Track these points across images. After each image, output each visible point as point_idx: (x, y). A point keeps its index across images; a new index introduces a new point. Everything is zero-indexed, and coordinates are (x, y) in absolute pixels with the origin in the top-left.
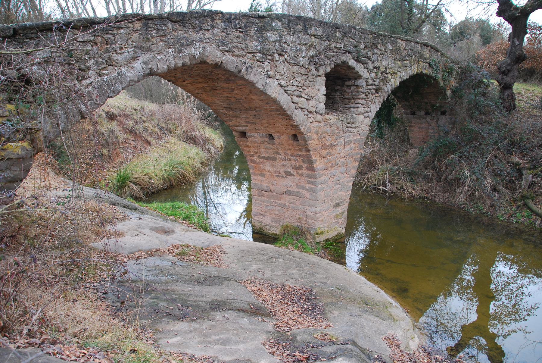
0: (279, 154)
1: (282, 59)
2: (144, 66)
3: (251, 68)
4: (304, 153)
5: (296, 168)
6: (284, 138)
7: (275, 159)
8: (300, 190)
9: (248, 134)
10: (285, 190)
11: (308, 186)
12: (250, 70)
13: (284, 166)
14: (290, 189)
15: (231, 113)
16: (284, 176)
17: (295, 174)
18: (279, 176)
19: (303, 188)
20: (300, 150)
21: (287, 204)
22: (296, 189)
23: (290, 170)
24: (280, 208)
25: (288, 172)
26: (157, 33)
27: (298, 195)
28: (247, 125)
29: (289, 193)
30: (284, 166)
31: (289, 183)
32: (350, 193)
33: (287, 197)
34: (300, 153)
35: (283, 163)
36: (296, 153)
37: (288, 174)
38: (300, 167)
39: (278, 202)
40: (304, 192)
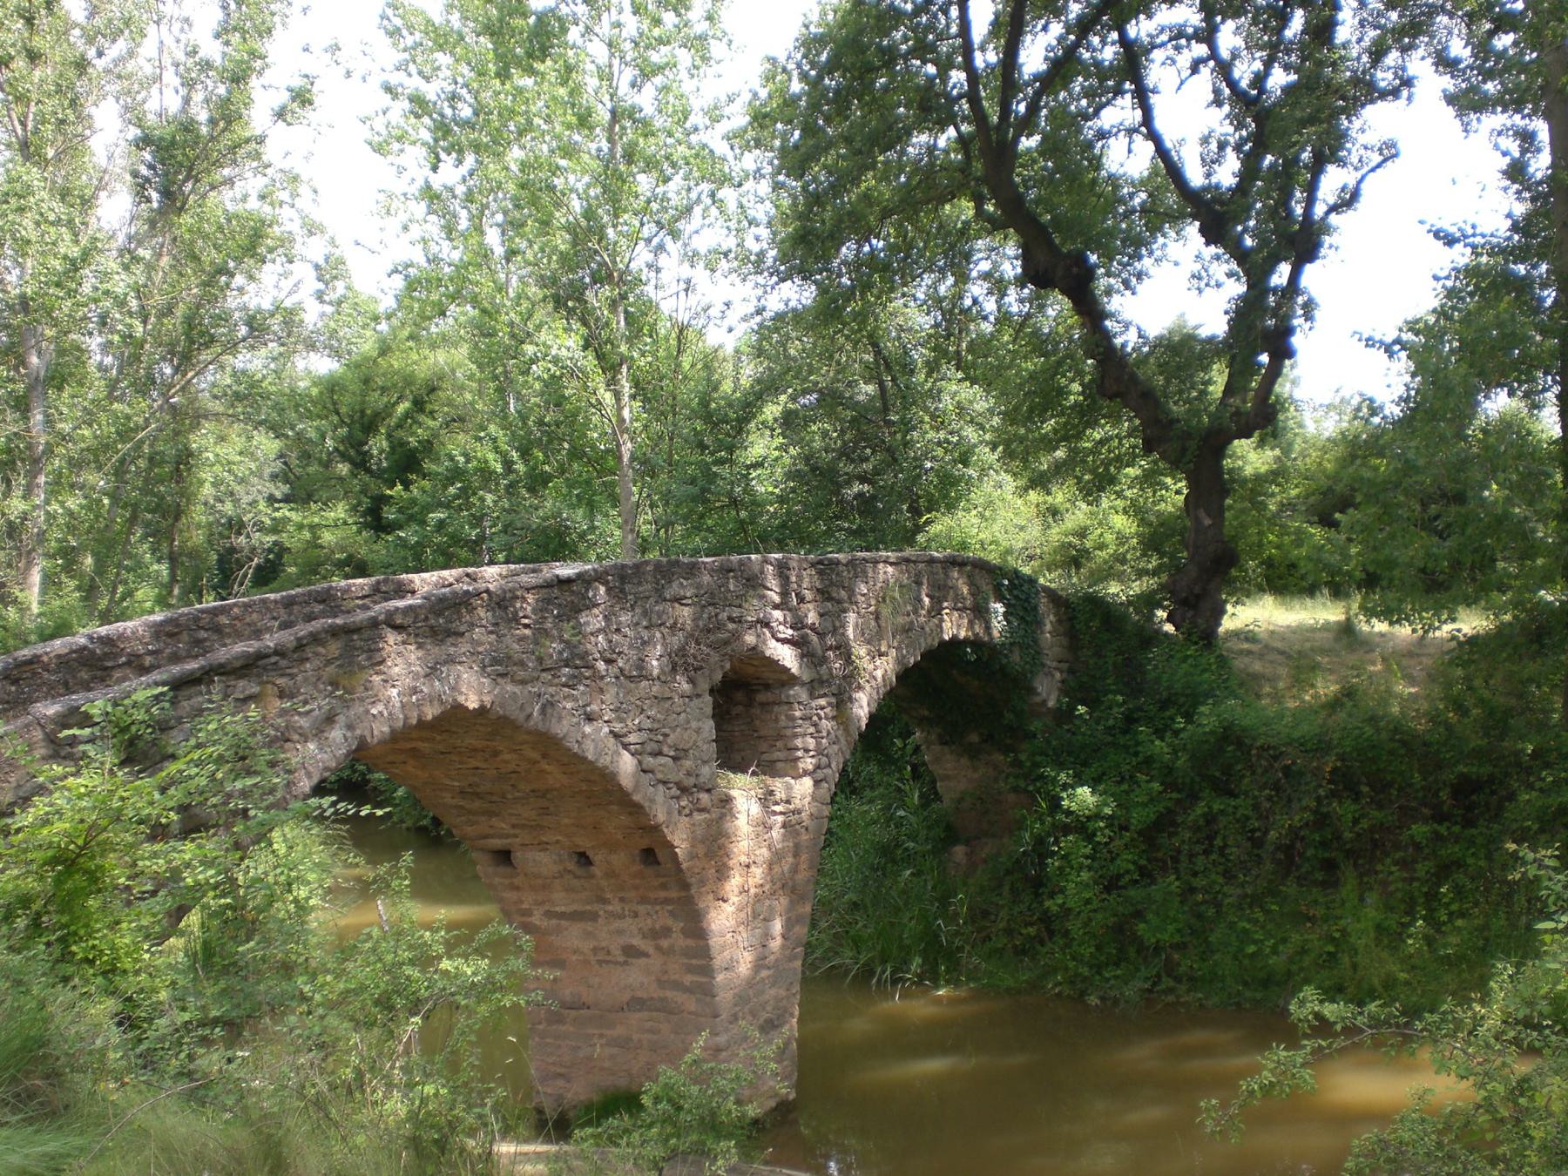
0: (605, 901)
1: (614, 670)
2: (349, 734)
3: (552, 704)
4: (674, 894)
5: (654, 934)
6: (619, 860)
7: (594, 917)
8: (669, 994)
9: (518, 856)
10: (626, 996)
11: (688, 979)
12: (549, 711)
13: (620, 932)
14: (639, 994)
15: (477, 804)
16: (621, 959)
17: (651, 951)
18: (607, 962)
19: (677, 985)
20: (664, 887)
21: (635, 1037)
22: (661, 993)
23: (637, 942)
24: (614, 1050)
25: (632, 947)
26: (369, 658)
27: (665, 1008)
28: (517, 831)
29: (637, 1004)
30: (620, 932)
31: (636, 978)
32: (797, 988)
33: (635, 1018)
34: (662, 894)
35: (617, 924)
36: (652, 896)
37: (631, 952)
38: (666, 932)
39: (608, 1032)
40: (678, 997)
